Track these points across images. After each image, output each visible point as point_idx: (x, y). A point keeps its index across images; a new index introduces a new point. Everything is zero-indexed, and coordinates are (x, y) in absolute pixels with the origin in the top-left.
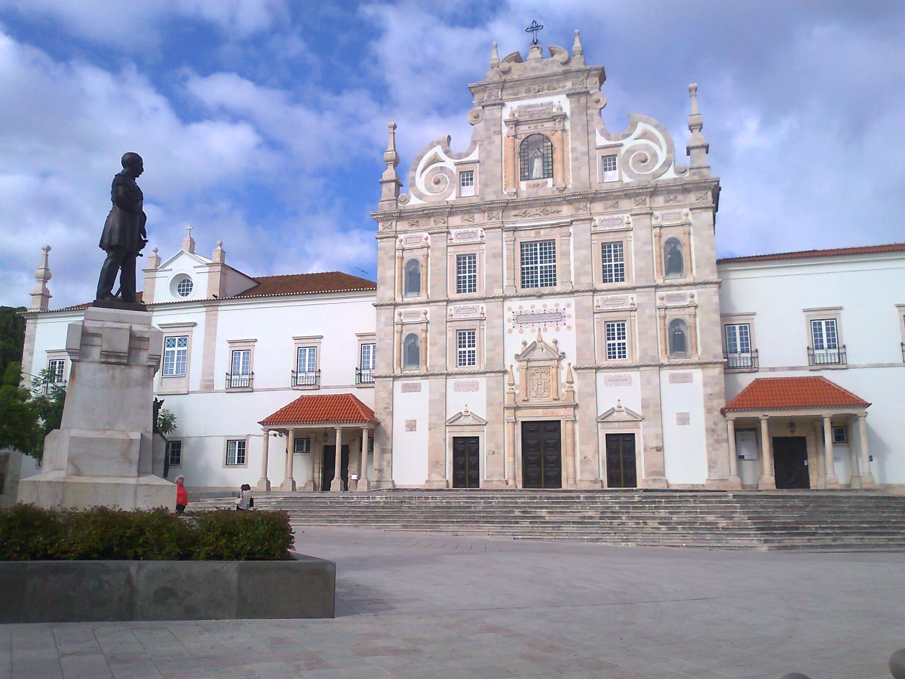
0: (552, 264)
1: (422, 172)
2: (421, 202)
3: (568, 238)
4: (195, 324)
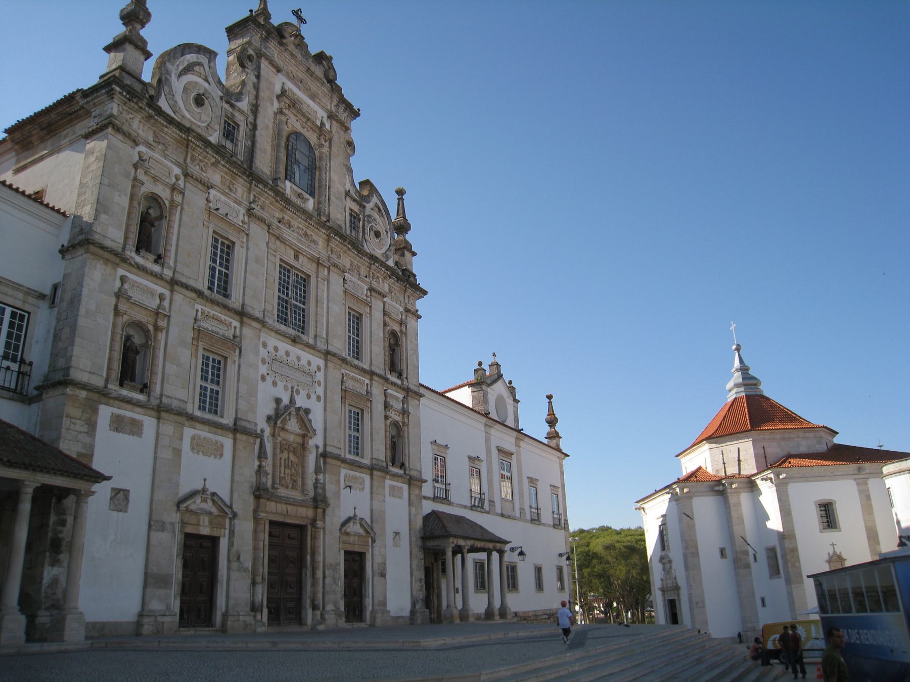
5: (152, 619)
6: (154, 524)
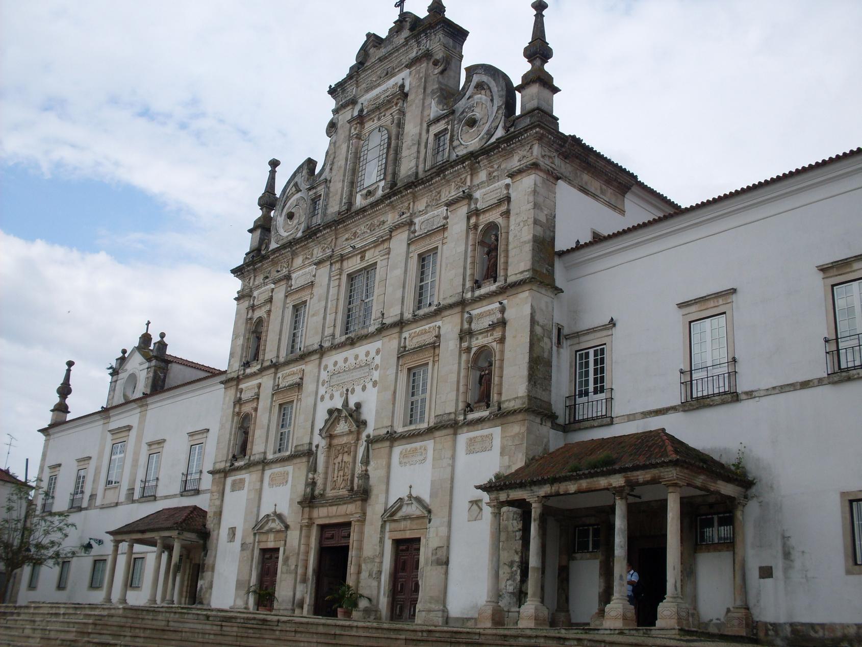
3: (387, 256)
4: (129, 428)
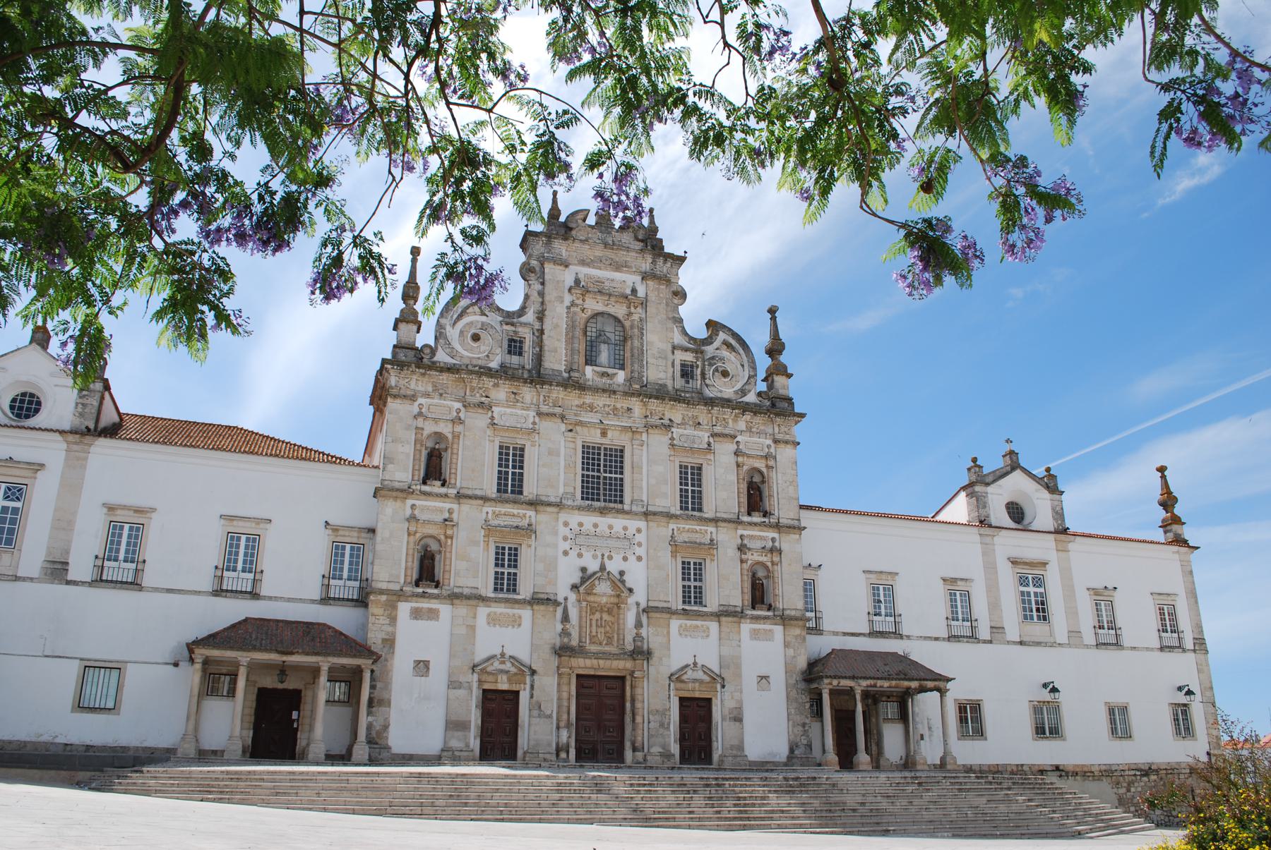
0: (618, 476)
1: (454, 324)
2: (454, 362)
5: (450, 753)
6: (453, 684)
